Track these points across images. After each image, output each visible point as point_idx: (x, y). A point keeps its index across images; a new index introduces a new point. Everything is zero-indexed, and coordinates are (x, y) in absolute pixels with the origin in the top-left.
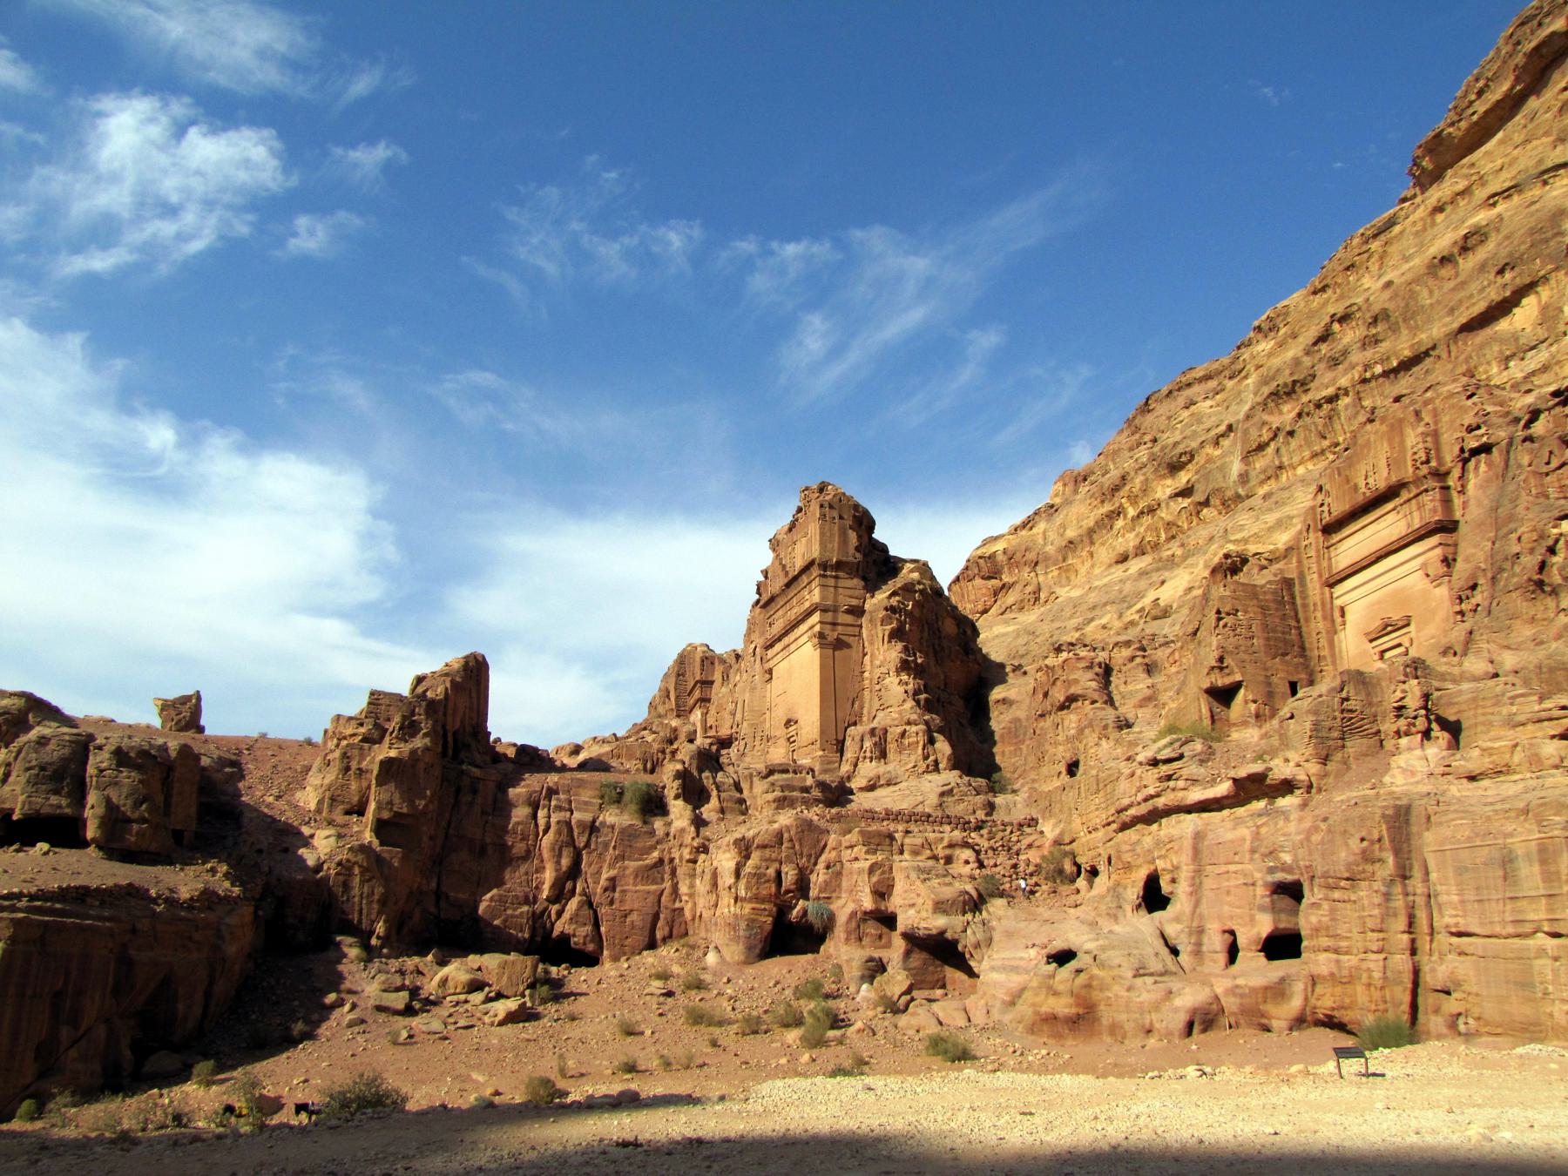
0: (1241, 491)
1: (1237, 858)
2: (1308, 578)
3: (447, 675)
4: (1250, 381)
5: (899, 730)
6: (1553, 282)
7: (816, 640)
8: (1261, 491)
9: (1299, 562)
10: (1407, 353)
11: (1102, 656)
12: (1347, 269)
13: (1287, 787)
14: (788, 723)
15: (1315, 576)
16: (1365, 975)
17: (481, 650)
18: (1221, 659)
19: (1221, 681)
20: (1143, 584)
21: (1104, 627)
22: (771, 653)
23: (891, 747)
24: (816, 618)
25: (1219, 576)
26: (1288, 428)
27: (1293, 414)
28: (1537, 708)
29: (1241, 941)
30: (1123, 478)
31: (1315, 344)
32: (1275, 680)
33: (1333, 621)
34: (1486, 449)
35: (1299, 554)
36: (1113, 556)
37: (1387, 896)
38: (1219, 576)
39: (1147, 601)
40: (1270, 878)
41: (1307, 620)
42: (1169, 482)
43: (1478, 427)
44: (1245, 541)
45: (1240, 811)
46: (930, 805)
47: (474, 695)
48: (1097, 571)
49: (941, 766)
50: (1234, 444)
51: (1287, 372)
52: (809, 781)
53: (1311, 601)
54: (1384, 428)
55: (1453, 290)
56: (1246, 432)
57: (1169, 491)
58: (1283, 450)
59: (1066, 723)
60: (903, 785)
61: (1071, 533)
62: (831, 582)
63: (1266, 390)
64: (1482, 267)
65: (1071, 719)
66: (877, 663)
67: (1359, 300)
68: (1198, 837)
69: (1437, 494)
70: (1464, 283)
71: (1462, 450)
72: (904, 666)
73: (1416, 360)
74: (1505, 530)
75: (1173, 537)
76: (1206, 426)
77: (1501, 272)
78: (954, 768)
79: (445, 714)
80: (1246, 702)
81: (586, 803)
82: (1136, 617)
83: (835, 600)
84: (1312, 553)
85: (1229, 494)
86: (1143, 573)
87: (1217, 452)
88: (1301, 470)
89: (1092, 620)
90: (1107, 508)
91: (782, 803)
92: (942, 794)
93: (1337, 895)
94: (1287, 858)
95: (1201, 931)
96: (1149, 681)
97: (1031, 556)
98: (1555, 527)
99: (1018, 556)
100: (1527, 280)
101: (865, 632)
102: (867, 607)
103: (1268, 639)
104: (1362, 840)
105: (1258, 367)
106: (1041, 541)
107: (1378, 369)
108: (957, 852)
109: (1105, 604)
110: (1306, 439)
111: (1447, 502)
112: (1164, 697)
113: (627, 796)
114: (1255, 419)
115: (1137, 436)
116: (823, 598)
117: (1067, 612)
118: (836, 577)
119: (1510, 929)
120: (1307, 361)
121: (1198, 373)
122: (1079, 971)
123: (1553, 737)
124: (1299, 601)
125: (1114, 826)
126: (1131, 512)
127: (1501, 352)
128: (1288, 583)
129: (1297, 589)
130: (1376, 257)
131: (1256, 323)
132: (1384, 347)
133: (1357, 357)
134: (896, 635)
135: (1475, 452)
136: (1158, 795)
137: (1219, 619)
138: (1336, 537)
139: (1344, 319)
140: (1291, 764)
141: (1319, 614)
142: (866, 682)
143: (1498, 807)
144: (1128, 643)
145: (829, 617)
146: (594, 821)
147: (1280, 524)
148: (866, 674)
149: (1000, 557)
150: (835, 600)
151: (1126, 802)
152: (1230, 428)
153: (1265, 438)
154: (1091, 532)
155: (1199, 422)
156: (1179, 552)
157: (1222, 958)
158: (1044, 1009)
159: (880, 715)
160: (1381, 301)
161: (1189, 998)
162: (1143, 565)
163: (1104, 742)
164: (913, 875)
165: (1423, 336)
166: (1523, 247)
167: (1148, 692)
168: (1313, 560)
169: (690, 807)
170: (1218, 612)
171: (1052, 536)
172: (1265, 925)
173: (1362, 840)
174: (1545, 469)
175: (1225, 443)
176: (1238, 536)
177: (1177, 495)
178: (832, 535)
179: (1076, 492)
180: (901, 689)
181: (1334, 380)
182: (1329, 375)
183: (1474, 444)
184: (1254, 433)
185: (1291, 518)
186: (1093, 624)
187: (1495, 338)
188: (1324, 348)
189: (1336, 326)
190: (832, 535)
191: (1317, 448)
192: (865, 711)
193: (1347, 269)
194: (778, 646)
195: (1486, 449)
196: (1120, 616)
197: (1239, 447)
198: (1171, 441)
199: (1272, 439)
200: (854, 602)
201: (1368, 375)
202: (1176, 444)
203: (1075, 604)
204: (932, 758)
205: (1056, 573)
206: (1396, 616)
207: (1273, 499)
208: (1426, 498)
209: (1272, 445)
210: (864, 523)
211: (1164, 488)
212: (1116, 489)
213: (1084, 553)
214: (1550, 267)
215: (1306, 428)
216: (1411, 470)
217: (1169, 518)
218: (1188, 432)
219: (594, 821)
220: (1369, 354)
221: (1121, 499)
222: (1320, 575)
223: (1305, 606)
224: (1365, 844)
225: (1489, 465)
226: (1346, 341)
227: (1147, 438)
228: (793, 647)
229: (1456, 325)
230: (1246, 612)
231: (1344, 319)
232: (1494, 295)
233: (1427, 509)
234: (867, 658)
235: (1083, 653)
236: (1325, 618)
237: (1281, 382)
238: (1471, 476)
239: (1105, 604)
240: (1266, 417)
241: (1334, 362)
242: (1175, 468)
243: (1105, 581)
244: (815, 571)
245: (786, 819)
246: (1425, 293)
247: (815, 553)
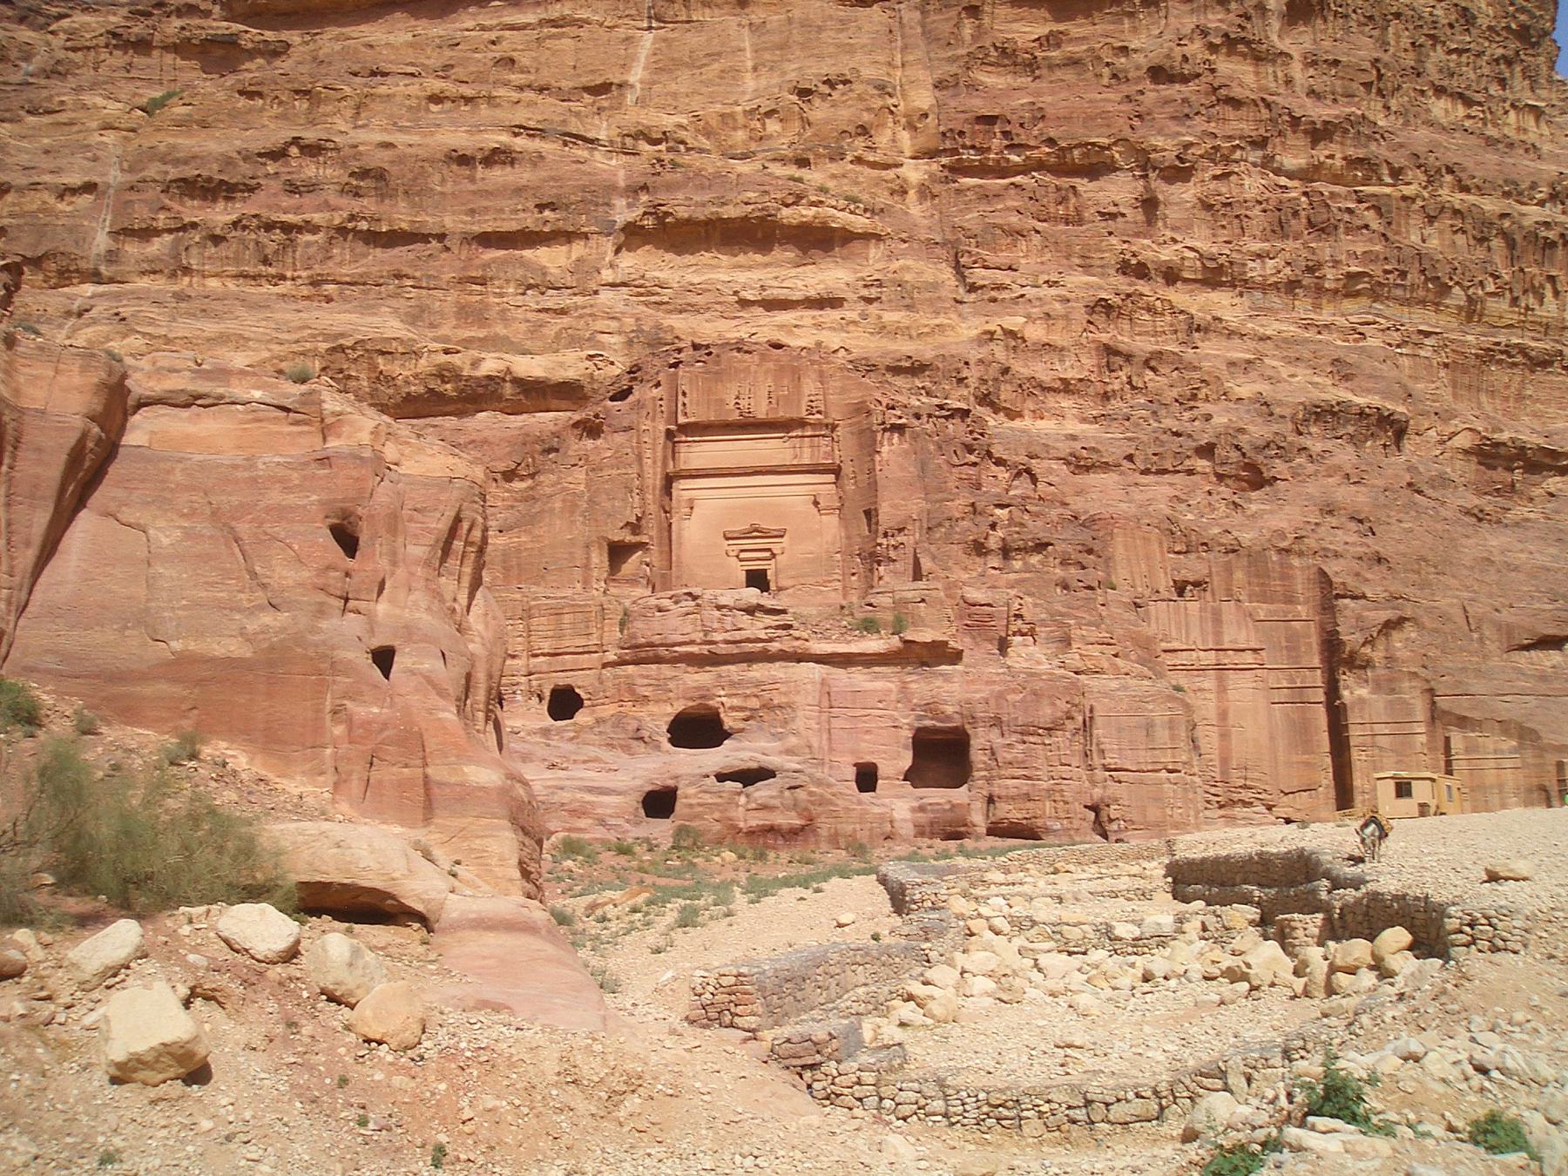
6: (592, 243)
26: (218, 232)
31: (260, 155)
40: (917, 724)
51: (215, 167)
58: (194, 251)
77: (541, 207)
85: (83, 265)
93: (1032, 739)
107: (364, 226)
120: (246, 169)
130: (351, 103)
136: (771, 640)
139: (313, 150)
147: (223, 339)
187: (523, 263)
188: (271, 168)
189: (294, 151)
199: (170, 231)
207: (196, 304)
229: (477, 229)
232: (530, 221)
237: (205, 173)
246: (437, 178)
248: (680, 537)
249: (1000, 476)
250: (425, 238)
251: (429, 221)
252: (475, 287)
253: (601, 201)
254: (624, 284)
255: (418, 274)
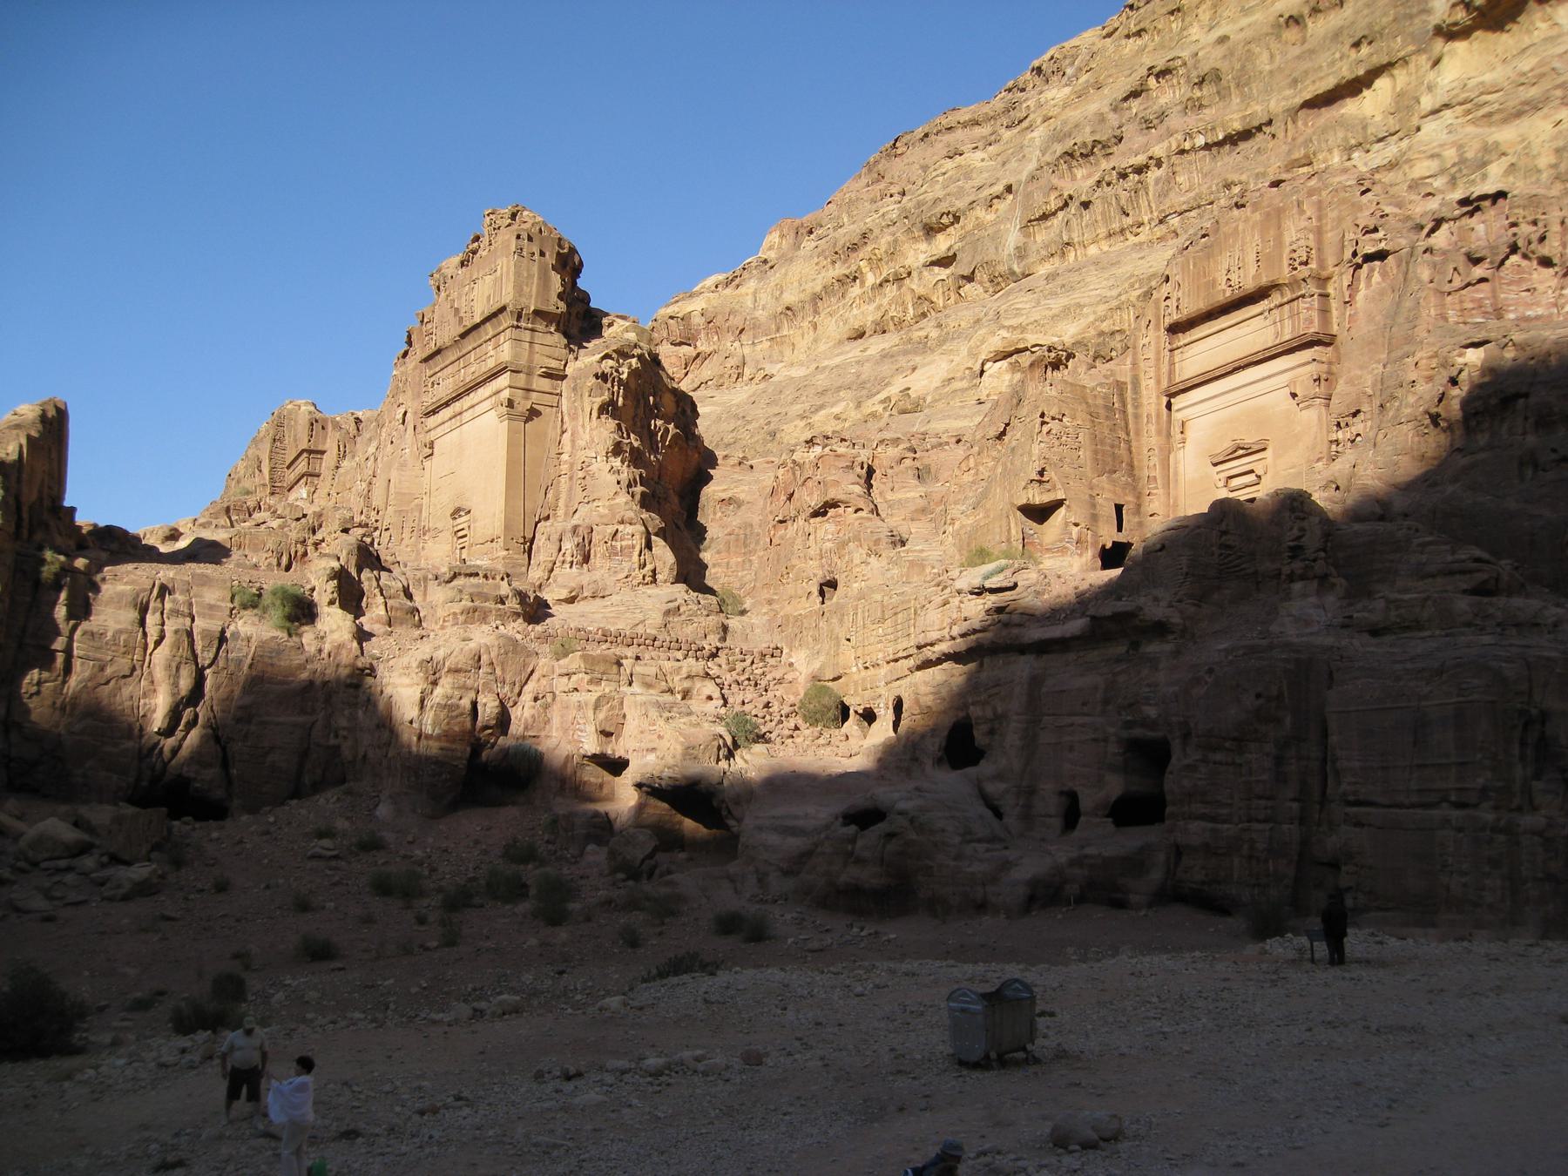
0: (1016, 268)
1: (1085, 709)
2: (1143, 384)
3: (18, 426)
4: (1035, 134)
5: (610, 529)
6: (1412, 66)
7: (504, 410)
8: (1043, 270)
9: (1134, 364)
10: (1237, 126)
11: (864, 455)
12: (1172, 13)
13: (1160, 629)
14: (456, 513)
15: (1152, 382)
16: (1246, 846)
17: (61, 397)
18: (1041, 473)
19: (1038, 497)
20: (886, 369)
21: (837, 418)
22: (432, 421)
23: (598, 551)
24: (504, 380)
25: (1038, 372)
26: (1084, 198)
27: (1092, 181)
28: (1450, 558)
29: (1086, 803)
30: (864, 236)
31: (1126, 99)
32: (1099, 500)
33: (1169, 435)
34: (1381, 256)
35: (1135, 354)
36: (845, 331)
37: (1279, 760)
38: (1038, 372)
39: (894, 390)
40: (1125, 734)
41: (1138, 433)
42: (923, 246)
43: (1376, 230)
44: (1022, 328)
45: (1094, 655)
46: (651, 627)
47: (54, 455)
48: (822, 347)
49: (659, 577)
50: (1012, 208)
51: (1088, 129)
52: (504, 589)
53: (1144, 411)
54: (1257, 216)
55: (1299, 57)
56: (1028, 196)
57: (922, 259)
58: (1074, 222)
59: (820, 534)
60: (614, 598)
61: (790, 298)
62: (527, 335)
63: (1059, 149)
64: (1336, 35)
65: (826, 528)
66: (582, 443)
67: (1185, 54)
68: (1035, 681)
69: (1316, 300)
70: (1312, 52)
71: (1355, 254)
72: (617, 450)
73: (1246, 135)
74: (1399, 353)
75: (924, 315)
76: (977, 183)
78: (677, 581)
79: (19, 481)
80: (1066, 524)
81: (211, 607)
82: (880, 408)
83: (530, 360)
84: (1151, 355)
85: (1002, 268)
86: (885, 356)
87: (990, 217)
88: (1093, 250)
89: (822, 407)
90: (840, 270)
91: (474, 615)
92: (667, 613)
93: (1218, 757)
94: (1151, 712)
95: (1031, 792)
96: (922, 490)
97: (737, 321)
98: (1460, 355)
99: (719, 321)
100: (1385, 60)
101: (564, 401)
102: (569, 371)
103: (1096, 452)
104: (1258, 696)
105: (1047, 119)
106: (749, 303)
107: (1200, 141)
108: (698, 684)
109: (839, 389)
110: (1103, 214)
111: (1325, 311)
112: (955, 511)
113: (267, 599)
114: (1042, 181)
115: (882, 185)
116: (516, 356)
117: (789, 394)
118: (532, 330)
119: (1415, 799)
121: (964, 115)
122: (890, 836)
123: (1465, 592)
124: (1130, 409)
125: (911, 662)
126: (871, 279)
127: (1346, 139)
128: (1120, 386)
129: (1129, 394)
131: (1036, 63)
132: (1208, 113)
133: (1175, 121)
134: (607, 408)
135: (1369, 258)
137: (1043, 423)
138: (1184, 338)
140: (1163, 604)
141: (1153, 428)
142: (564, 468)
143: (1409, 666)
144: (896, 441)
145: (521, 379)
146: (223, 632)
147: (1066, 313)
148: (565, 457)
149: (697, 320)
150: (530, 360)
151: (934, 636)
152: (1009, 189)
153: (1053, 206)
154: (817, 298)
155: (968, 176)
156: (934, 334)
157: (1057, 823)
158: (843, 878)
159: (583, 510)
160: (1212, 58)
161: (1030, 866)
162: (886, 345)
163: (873, 560)
164: (653, 713)
165: (1258, 108)
166: (1385, 20)
167: (922, 503)
168: (1152, 363)
169: (351, 617)
170: (1042, 415)
171: (764, 298)
172: (1115, 786)
173: (1258, 696)
174: (1447, 288)
175: (1001, 206)
176: (1014, 322)
177: (933, 264)
178: (530, 276)
179: (797, 246)
180: (613, 478)
181: (1146, 147)
182: (1140, 140)
183: (1370, 250)
184: (1038, 198)
185: (1080, 306)
186: (823, 412)
187: (1342, 123)
188: (1135, 105)
189: (1152, 81)
190: (530, 276)
191: (1116, 226)
192: (561, 503)
193: (1172, 13)
194: (445, 413)
195: (1381, 256)
196: (859, 405)
197: (1018, 212)
198: (930, 196)
199: (1061, 209)
200: (554, 364)
201: (1187, 146)
202: (937, 201)
203: (801, 386)
204: (649, 567)
205: (766, 344)
206: (1249, 439)
207: (1059, 281)
208: (1301, 304)
209: (1060, 214)
210: (569, 264)
211: (918, 253)
212: (854, 248)
213: (805, 324)
214: (1411, 48)
215: (1104, 199)
216: (1286, 269)
217: (921, 291)
218: (952, 188)
219: (223, 632)
220: (1192, 121)
221: (859, 261)
222: (1158, 382)
223: (1137, 416)
224: (1261, 701)
225: (1384, 274)
226: (1163, 101)
227: (895, 190)
228: (467, 416)
229: (1298, 101)
230: (1074, 418)
231: (1163, 74)
232: (1347, 71)
233: (1305, 318)
234: (567, 436)
235: (841, 449)
236: (1159, 432)
237: (1079, 140)
238: (1362, 285)
239: (839, 389)
240: (1055, 181)
241: (1148, 125)
242: (931, 230)
243: (838, 360)
244: (506, 320)
245: (483, 636)
246: (1265, 56)
247: (507, 296)
248: (1176, 474)
249: (1541, 288)
250: (1259, 129)
251: (1258, 111)
252: (1301, 170)
253: (1415, 10)
254: (1447, 106)
255: (1244, 178)
